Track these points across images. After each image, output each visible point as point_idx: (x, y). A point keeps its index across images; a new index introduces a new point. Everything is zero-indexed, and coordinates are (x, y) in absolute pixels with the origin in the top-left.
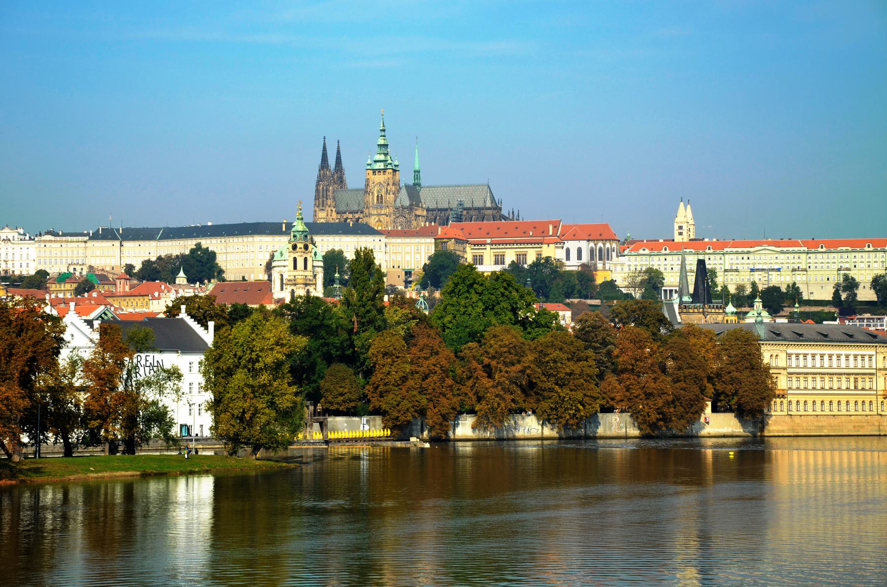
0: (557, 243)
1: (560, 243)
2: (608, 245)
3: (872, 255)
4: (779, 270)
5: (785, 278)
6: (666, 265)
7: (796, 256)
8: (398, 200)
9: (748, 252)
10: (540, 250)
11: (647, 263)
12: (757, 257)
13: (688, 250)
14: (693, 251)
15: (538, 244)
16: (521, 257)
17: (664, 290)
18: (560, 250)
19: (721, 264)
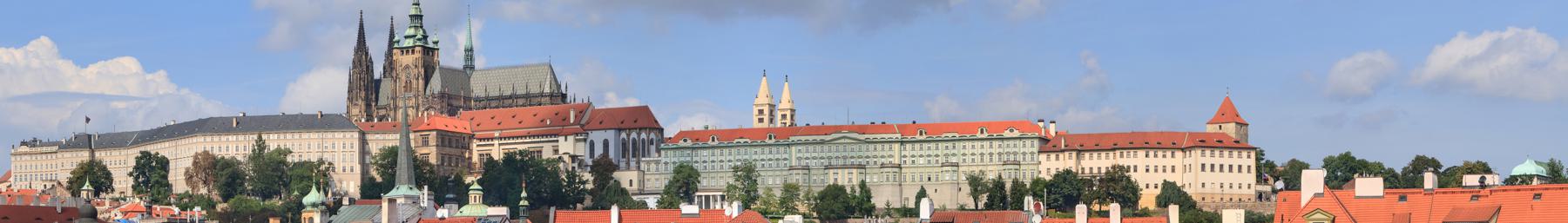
0: (577, 134)
1: (581, 135)
2: (644, 135)
3: (986, 144)
4: (861, 167)
5: (871, 178)
6: (713, 162)
7: (887, 146)
8: (429, 86)
9: (822, 142)
11: (689, 159)
12: (834, 148)
13: (742, 141)
14: (750, 142)
15: (555, 135)
16: (536, 155)
17: (698, 196)
19: (785, 159)
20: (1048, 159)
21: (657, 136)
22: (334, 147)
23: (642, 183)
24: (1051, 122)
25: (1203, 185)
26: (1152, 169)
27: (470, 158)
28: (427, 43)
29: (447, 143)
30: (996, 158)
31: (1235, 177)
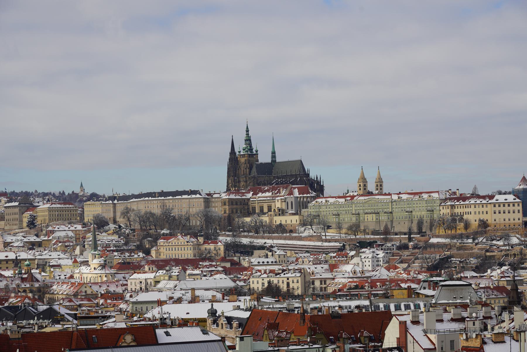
5: (382, 218)
6: (326, 211)
10: (274, 203)
11: (318, 210)
18: (284, 203)
19: (351, 210)
20: (443, 209)
21: (311, 199)
22: (194, 206)
23: (302, 221)
24: (458, 190)
25: (495, 220)
26: (477, 213)
27: (248, 209)
28: (252, 152)
29: (234, 203)
30: (424, 208)
31: (512, 216)
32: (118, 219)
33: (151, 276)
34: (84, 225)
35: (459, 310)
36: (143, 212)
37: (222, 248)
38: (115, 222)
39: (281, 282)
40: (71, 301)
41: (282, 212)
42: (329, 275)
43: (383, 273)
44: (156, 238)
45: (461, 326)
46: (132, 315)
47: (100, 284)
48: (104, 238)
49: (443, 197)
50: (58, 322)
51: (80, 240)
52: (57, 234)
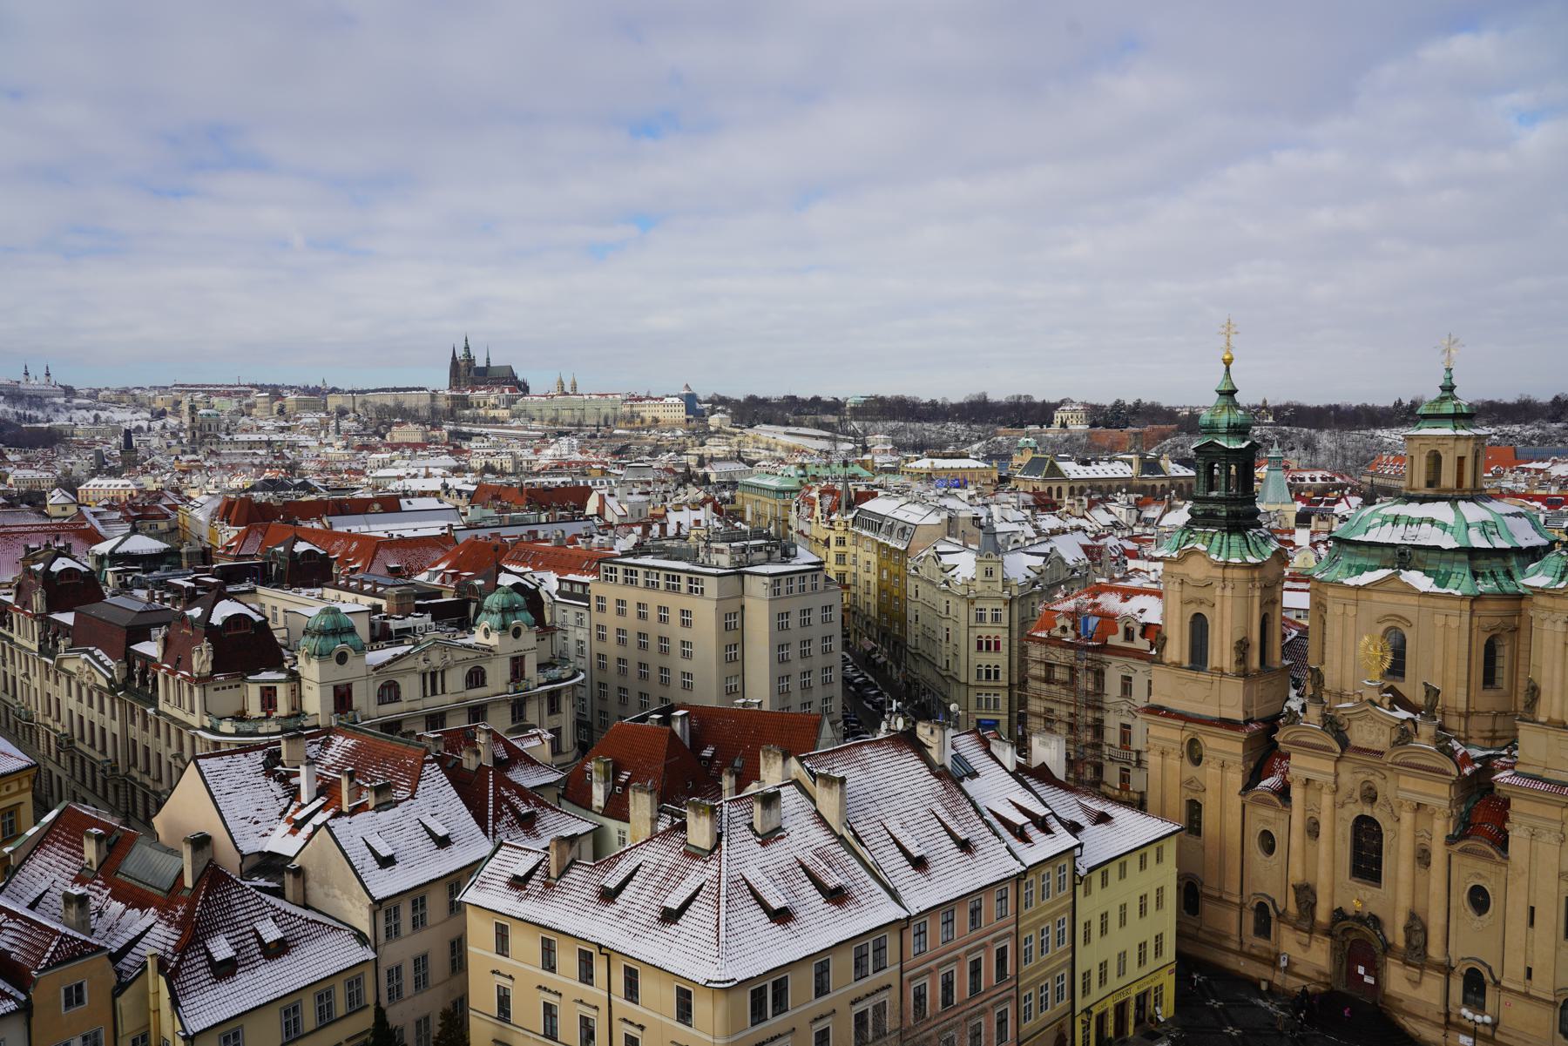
32: (357, 409)
33: (388, 456)
34: (328, 413)
35: (645, 486)
36: (378, 404)
37: (446, 435)
38: (354, 411)
39: (495, 462)
40: (319, 475)
41: (495, 407)
42: (534, 457)
43: (577, 457)
44: (390, 426)
45: (647, 498)
46: (377, 488)
47: (343, 462)
48: (345, 424)
49: (624, 398)
50: (313, 493)
51: (324, 425)
52: (304, 421)
